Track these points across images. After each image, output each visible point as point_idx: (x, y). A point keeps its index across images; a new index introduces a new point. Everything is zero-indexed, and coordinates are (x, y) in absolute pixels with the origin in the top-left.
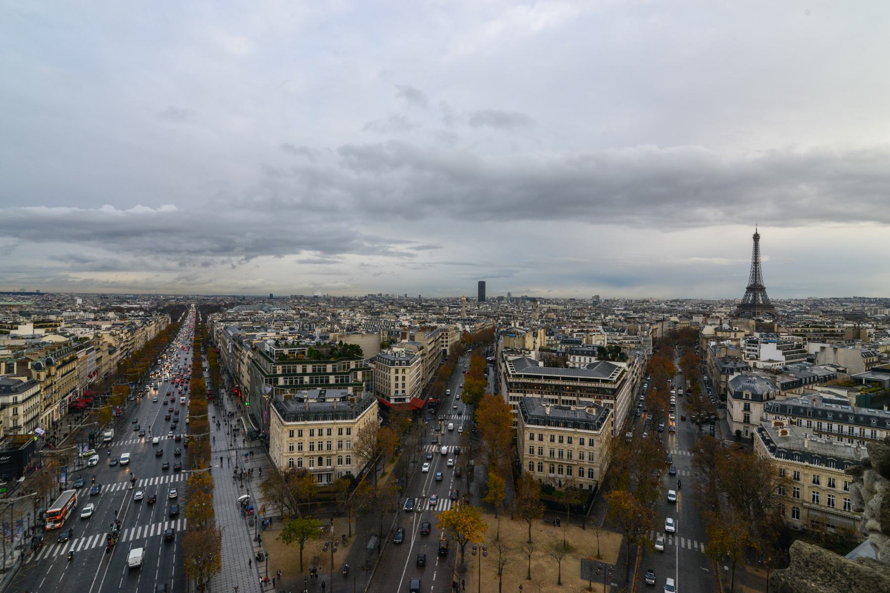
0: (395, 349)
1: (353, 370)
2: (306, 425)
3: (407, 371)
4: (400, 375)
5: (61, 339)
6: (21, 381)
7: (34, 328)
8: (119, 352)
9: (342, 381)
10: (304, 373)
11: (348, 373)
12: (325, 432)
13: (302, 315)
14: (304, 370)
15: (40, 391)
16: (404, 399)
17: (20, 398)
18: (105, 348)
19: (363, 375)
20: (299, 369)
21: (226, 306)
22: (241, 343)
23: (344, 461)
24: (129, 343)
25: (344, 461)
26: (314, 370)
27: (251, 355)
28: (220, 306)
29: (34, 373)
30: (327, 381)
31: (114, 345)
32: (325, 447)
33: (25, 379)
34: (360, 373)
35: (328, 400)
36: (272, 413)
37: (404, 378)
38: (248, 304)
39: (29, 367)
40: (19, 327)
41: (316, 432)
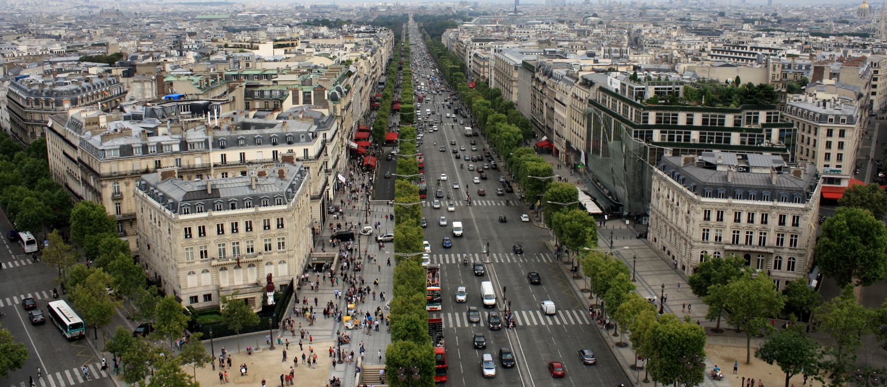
0: (821, 96)
1: (763, 125)
2: (730, 204)
3: (847, 134)
4: (835, 139)
5: (328, 62)
6: (323, 115)
8: (369, 82)
9: (751, 141)
10: (690, 126)
11: (760, 131)
12: (758, 218)
13: (581, 33)
14: (690, 121)
16: (838, 181)
17: (329, 137)
18: (363, 76)
19: (781, 138)
21: (455, 16)
22: (550, 75)
23: (784, 264)
25: (784, 264)
26: (705, 121)
28: (447, 17)
29: (331, 103)
30: (728, 140)
32: (756, 241)
33: (326, 112)
34: (775, 132)
35: (754, 171)
36: (655, 185)
37: (841, 145)
39: (326, 98)
40: (261, 46)
41: (744, 217)
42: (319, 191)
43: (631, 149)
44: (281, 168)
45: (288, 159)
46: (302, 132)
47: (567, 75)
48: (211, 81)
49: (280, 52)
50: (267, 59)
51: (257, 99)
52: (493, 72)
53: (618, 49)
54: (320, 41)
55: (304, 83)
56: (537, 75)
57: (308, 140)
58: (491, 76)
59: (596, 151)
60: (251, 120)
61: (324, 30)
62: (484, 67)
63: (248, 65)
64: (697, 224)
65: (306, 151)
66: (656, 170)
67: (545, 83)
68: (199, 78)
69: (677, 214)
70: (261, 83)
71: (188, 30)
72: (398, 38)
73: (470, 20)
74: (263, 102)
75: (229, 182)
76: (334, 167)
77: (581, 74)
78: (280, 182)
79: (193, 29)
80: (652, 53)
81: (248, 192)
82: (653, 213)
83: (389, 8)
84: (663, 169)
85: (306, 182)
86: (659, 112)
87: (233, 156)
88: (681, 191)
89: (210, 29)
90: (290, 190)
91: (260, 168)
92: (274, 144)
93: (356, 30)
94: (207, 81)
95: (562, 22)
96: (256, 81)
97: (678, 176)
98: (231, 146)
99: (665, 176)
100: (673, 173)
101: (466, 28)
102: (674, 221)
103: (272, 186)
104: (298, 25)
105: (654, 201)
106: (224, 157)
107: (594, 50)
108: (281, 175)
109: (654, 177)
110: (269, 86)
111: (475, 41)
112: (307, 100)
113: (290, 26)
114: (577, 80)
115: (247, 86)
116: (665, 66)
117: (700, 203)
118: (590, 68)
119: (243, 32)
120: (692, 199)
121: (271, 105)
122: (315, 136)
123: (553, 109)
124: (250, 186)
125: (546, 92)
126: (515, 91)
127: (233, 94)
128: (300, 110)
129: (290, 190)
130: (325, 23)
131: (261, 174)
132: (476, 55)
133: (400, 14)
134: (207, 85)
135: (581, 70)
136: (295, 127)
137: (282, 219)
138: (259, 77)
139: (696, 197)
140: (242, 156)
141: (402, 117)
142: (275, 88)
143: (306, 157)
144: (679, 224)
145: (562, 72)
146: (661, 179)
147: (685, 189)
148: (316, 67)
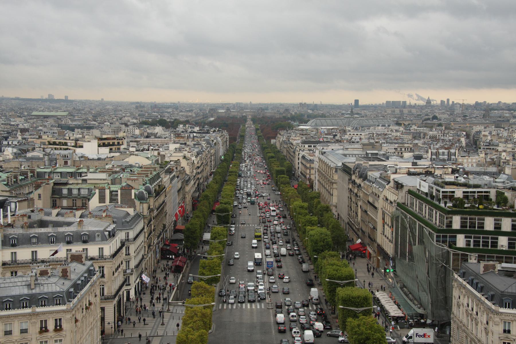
6: (128, 214)
7: (99, 146)
8: (192, 182)
10: (498, 231)
13: (416, 136)
14: (498, 227)
15: (143, 229)
17: (132, 236)
20: (489, 224)
21: (293, 118)
22: (364, 177)
24: (199, 170)
27: (392, 197)
28: (286, 119)
29: (137, 202)
31: (188, 172)
36: (456, 293)
38: (323, 116)
39: (133, 197)
40: (85, 144)
42: (114, 292)
43: (433, 254)
44: (64, 267)
45: (77, 258)
46: (98, 231)
47: (380, 178)
48: (20, 177)
49: (105, 152)
50: (91, 157)
51: (65, 197)
52: (317, 173)
53: (446, 151)
54: (152, 140)
55: (113, 182)
56: (353, 177)
57: (104, 239)
58: (315, 177)
59: (403, 255)
60: (53, 218)
61: (159, 130)
62: (311, 168)
63: (66, 163)
64: (496, 337)
65: (101, 250)
66: (456, 276)
67: (360, 185)
68: (6, 175)
69: (477, 325)
70: (71, 182)
71: (21, 126)
72: (232, 139)
73: (306, 122)
74: (71, 201)
75: (8, 281)
76: (137, 266)
77: (393, 176)
78: (62, 281)
79: (26, 126)
80: (483, 155)
81: (26, 291)
82: (455, 322)
83: (228, 109)
84: (463, 275)
85: (95, 282)
86: (465, 216)
87: (24, 254)
88: (479, 300)
89: (45, 126)
90: (72, 290)
91: (43, 267)
92: (69, 243)
93: (190, 130)
94: (16, 177)
95: (398, 124)
96: (64, 180)
97: (477, 283)
98: (23, 244)
99: (465, 283)
100: (472, 280)
101: (302, 130)
102: (474, 332)
103: (54, 285)
104: (134, 124)
105: (454, 309)
106: (14, 254)
107: (421, 153)
108: (65, 275)
109: (455, 284)
110: (77, 184)
111: (304, 142)
112: (113, 199)
113: (126, 125)
114: (389, 182)
115: (55, 184)
116: (493, 169)
117: (498, 313)
118: (406, 171)
119: (76, 130)
120: (490, 309)
121: (79, 203)
122: (112, 235)
123: (366, 212)
124: (29, 286)
125: (361, 194)
126: (335, 193)
127: (40, 191)
128: (104, 209)
129: (72, 290)
130: (163, 123)
131: (43, 273)
132: (303, 157)
133: (239, 115)
134: (16, 182)
135: (396, 173)
136: (91, 225)
137: (60, 320)
138: (72, 175)
139: (493, 307)
140: (34, 253)
141: (219, 217)
142: (84, 186)
143: (101, 257)
144: (479, 336)
145: (376, 174)
146: (461, 286)
147: (483, 298)
148: (131, 166)
